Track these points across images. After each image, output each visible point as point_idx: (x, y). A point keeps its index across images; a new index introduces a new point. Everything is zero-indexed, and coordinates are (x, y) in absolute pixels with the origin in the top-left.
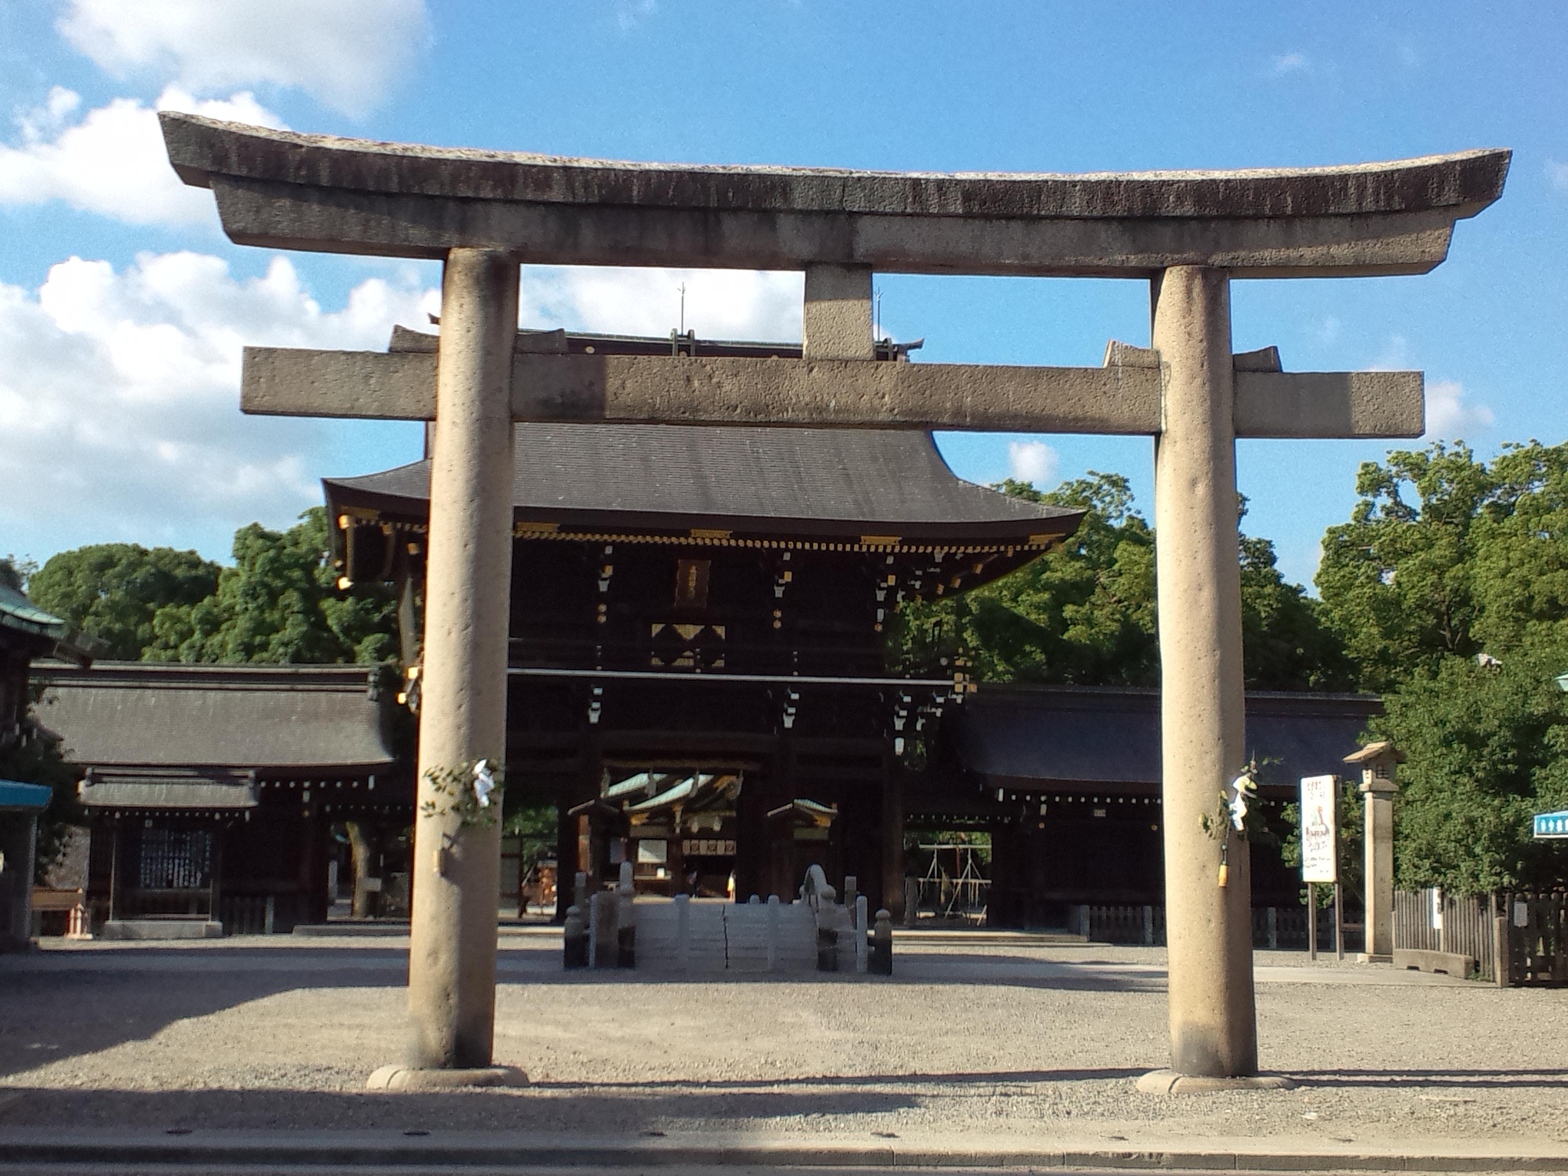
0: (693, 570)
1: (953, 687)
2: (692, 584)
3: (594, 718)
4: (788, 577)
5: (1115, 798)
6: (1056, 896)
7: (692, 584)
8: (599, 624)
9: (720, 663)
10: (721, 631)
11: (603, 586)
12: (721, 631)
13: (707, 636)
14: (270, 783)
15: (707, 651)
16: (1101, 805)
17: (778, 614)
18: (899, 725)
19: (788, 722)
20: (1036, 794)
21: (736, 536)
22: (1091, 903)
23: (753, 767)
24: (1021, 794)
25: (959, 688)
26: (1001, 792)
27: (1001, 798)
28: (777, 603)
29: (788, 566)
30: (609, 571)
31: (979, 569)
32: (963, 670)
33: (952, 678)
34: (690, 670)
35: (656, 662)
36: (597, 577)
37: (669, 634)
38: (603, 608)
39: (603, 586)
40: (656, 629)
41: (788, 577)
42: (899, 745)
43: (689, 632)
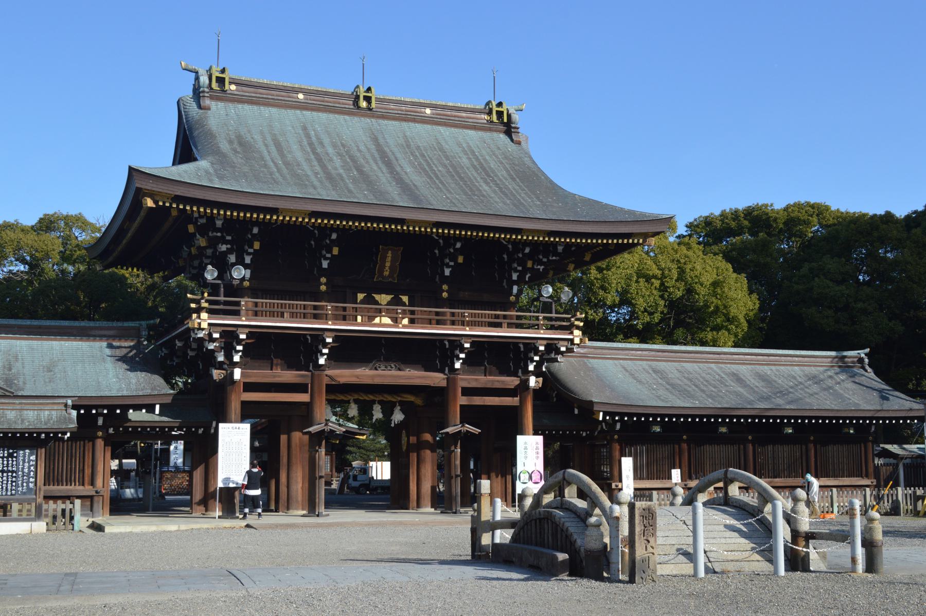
0: (390, 254)
1: (572, 341)
2: (388, 264)
7: (388, 264)
8: (321, 292)
10: (405, 299)
17: (445, 287)
18: (531, 368)
24: (612, 414)
25: (577, 341)
26: (601, 414)
27: (601, 419)
28: (445, 280)
31: (588, 257)
32: (578, 328)
33: (572, 333)
37: (370, 300)
38: (323, 280)
42: (533, 381)
43: (384, 299)
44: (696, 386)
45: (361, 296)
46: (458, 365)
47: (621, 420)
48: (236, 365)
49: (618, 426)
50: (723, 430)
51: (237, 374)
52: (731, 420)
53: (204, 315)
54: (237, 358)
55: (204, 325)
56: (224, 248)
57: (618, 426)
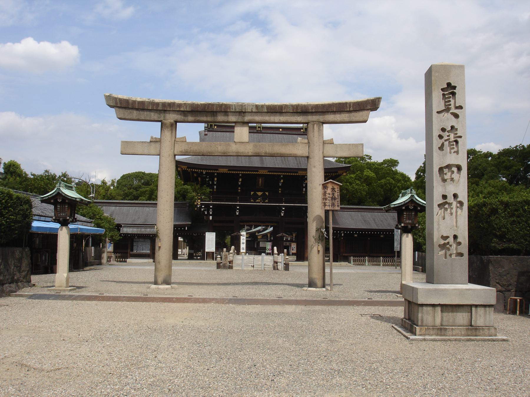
3: (237, 214)
4: (282, 181)
5: (359, 232)
6: (346, 255)
9: (267, 201)
10: (267, 193)
11: (240, 183)
12: (267, 193)
13: (264, 194)
14: (177, 228)
15: (264, 197)
16: (356, 233)
19: (282, 215)
20: (340, 231)
21: (269, 172)
22: (353, 257)
23: (276, 224)
29: (282, 178)
30: (240, 180)
34: (259, 203)
35: (252, 201)
36: (238, 181)
37: (255, 194)
39: (240, 183)
40: (252, 193)
41: (282, 181)
43: (260, 194)
44: (374, 221)
45: (252, 193)
46: (282, 215)
47: (344, 233)
48: (211, 215)
49: (343, 235)
50: (382, 236)
51: (211, 218)
52: (359, 232)
53: (199, 201)
54: (211, 213)
55: (199, 204)
56: (207, 180)
57: (343, 235)
